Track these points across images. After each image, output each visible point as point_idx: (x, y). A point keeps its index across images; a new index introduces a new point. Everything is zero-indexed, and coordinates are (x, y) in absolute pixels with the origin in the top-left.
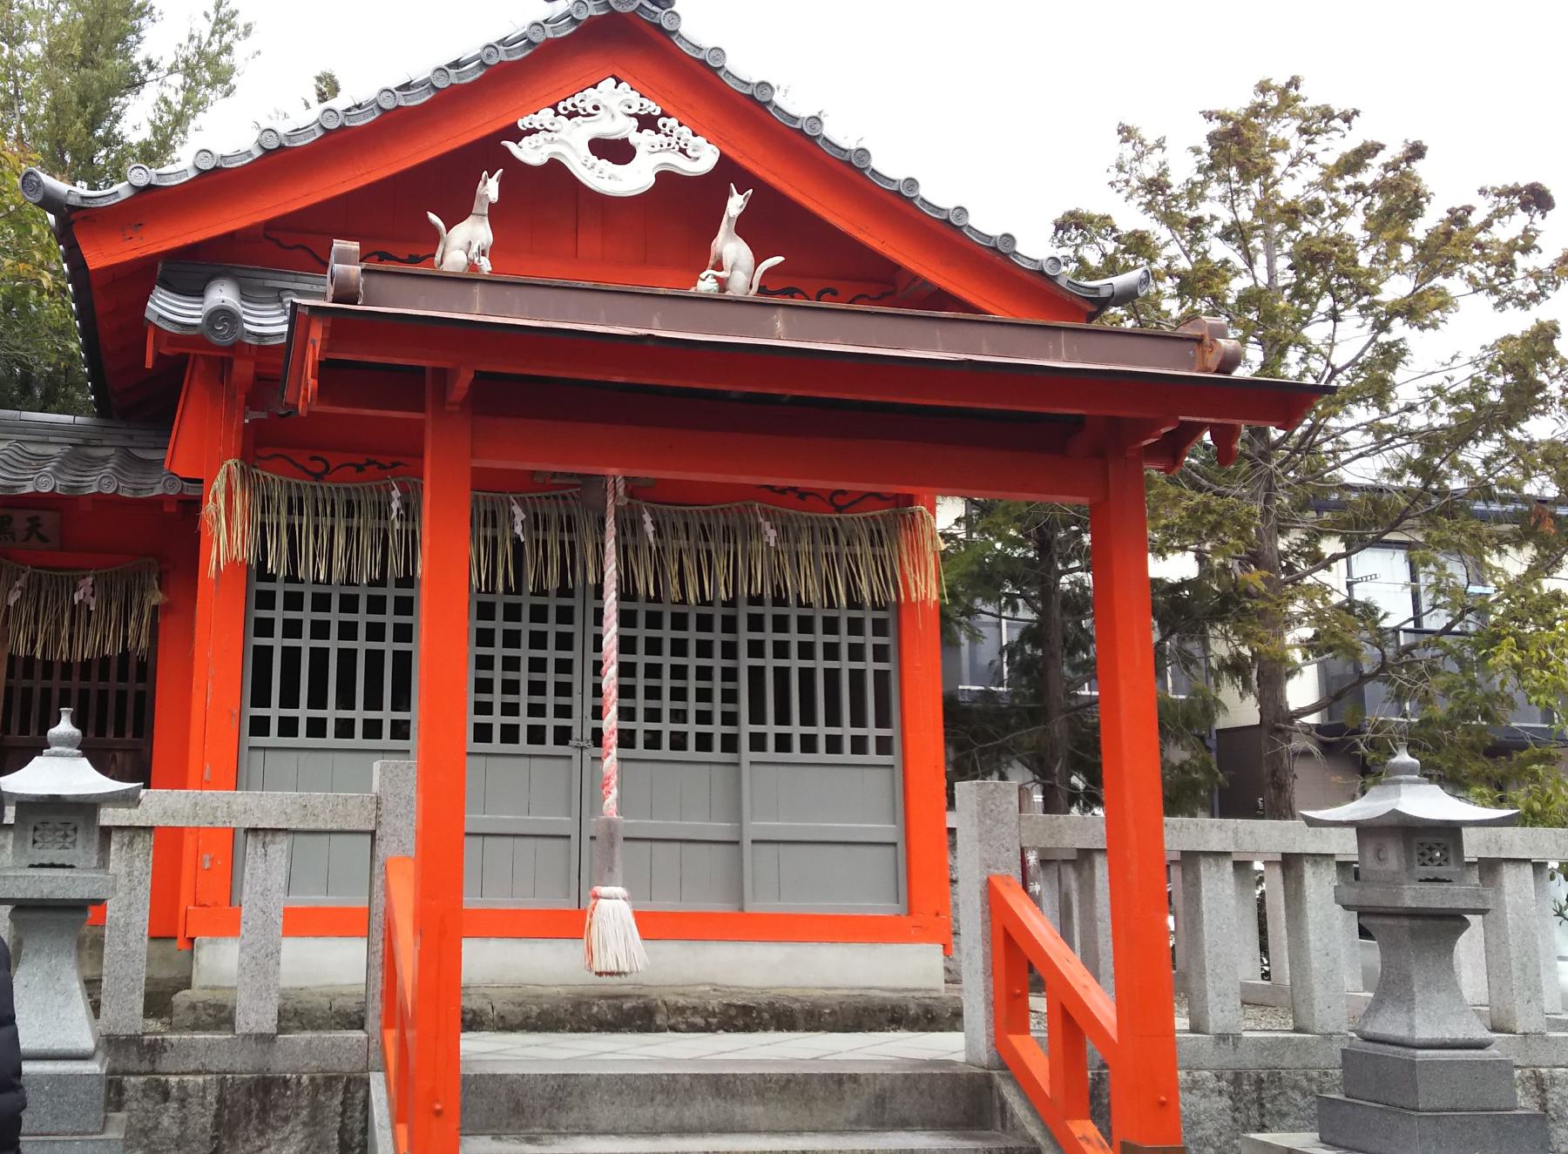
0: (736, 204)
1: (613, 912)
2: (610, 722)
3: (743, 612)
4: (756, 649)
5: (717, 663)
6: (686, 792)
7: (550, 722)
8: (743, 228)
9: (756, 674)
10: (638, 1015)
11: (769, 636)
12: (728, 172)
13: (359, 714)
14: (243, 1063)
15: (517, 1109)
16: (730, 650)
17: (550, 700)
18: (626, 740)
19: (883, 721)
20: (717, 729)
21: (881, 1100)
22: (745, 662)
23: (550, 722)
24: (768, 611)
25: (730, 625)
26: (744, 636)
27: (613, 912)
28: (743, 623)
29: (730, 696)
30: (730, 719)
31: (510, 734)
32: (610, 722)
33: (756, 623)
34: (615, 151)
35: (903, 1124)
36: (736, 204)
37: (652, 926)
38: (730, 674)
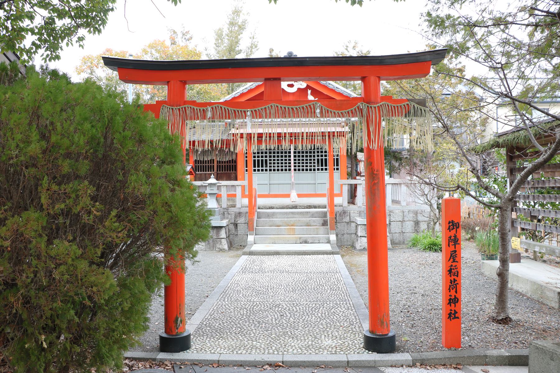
0: (309, 92)
1: (294, 194)
2: (292, 168)
3: (316, 150)
4: (318, 156)
5: (312, 158)
6: (306, 177)
7: (288, 168)
8: (312, 94)
9: (318, 160)
10: (295, 207)
11: (320, 154)
12: (308, 87)
13: (260, 168)
14: (238, 211)
15: (268, 216)
16: (314, 156)
17: (288, 165)
18: (295, 170)
19: (337, 165)
20: (312, 168)
21: (313, 215)
22: (316, 158)
23: (288, 168)
24: (320, 150)
25: (314, 152)
26: (316, 154)
27: (294, 194)
28: (316, 152)
29: (314, 163)
30: (314, 166)
31: (282, 170)
32: (292, 168)
33: (318, 152)
34: (291, 86)
35: (316, 217)
36: (309, 92)
37: (299, 196)
38: (314, 160)
